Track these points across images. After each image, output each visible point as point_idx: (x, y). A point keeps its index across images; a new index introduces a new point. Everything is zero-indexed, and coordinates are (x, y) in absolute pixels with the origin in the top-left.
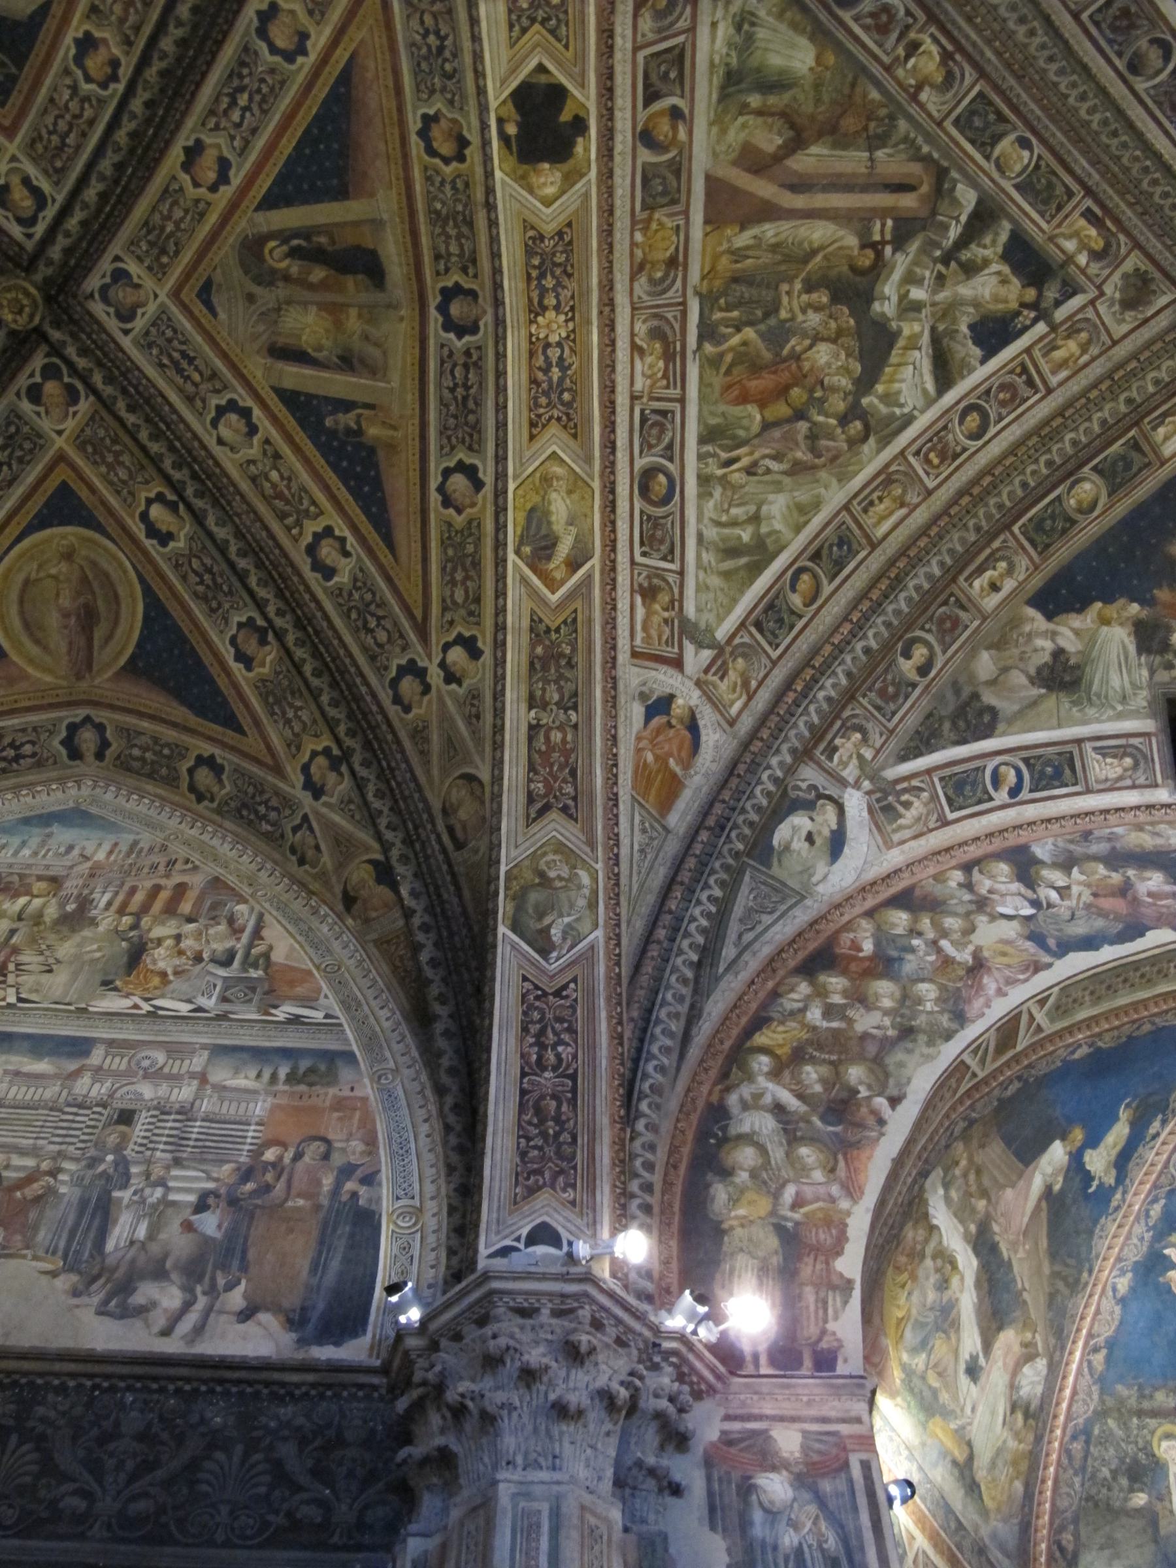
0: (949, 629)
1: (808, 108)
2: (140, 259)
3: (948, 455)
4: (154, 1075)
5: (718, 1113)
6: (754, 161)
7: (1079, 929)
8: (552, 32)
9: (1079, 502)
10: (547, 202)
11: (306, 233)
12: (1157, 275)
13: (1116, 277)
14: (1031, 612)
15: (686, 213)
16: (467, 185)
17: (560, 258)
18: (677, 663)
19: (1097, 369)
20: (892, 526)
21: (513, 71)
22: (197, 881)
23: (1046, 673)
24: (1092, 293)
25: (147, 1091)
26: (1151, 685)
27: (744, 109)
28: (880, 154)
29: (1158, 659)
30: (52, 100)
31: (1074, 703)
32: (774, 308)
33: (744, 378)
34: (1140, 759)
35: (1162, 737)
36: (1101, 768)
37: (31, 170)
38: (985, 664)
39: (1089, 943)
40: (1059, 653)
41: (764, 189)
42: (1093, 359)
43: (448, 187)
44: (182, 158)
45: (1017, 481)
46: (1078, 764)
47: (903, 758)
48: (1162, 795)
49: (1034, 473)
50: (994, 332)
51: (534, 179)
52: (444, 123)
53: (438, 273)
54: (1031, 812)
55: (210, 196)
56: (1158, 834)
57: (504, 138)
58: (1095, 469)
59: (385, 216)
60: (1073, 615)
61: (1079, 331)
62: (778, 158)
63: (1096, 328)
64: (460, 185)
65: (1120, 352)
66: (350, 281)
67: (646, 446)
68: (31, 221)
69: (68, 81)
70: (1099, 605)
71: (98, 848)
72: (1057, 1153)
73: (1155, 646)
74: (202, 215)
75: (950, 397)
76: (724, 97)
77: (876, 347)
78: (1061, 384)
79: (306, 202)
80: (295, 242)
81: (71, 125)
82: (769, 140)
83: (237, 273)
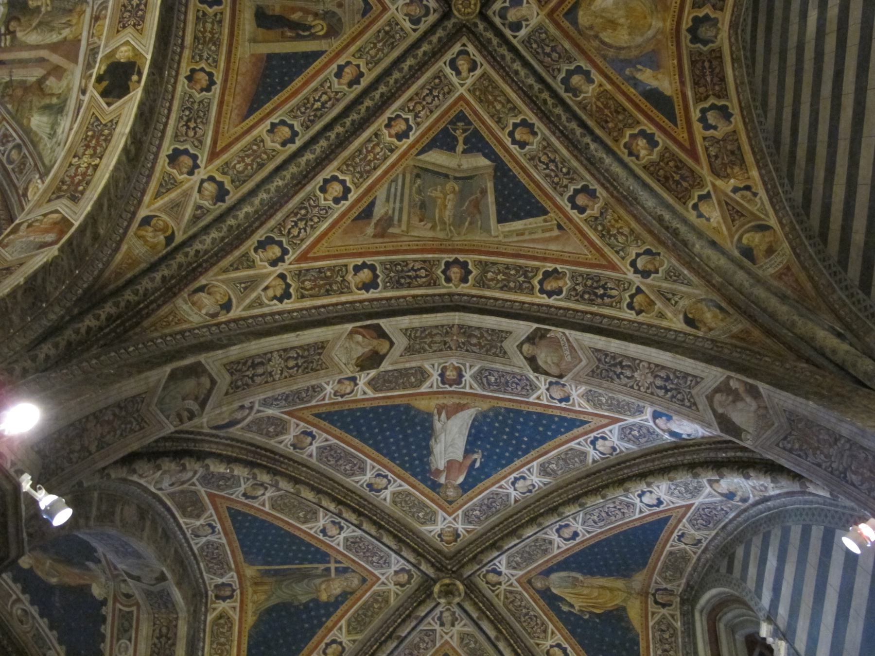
1: (35, 99)
2: (402, 29)
6: (57, 71)
8: (97, 119)
10: (127, 43)
11: (299, 38)
15: (88, 45)
16: (193, 57)
17: (127, 14)
21: (125, 103)
27: (59, 96)
28: (8, 79)
30: (431, 112)
37: (455, 79)
41: (55, 59)
43: (205, 55)
44: (362, 80)
51: (130, 54)
52: (198, 87)
53: (222, 13)
55: (351, 59)
57: (140, 74)
59: (247, 44)
62: (49, 74)
64: (198, 58)
66: (277, 11)
68: (460, 53)
69: (419, 120)
74: (359, 50)
76: (65, 101)
79: (296, 53)
80: (306, 33)
81: (424, 99)
82: (51, 82)
83: (345, 19)
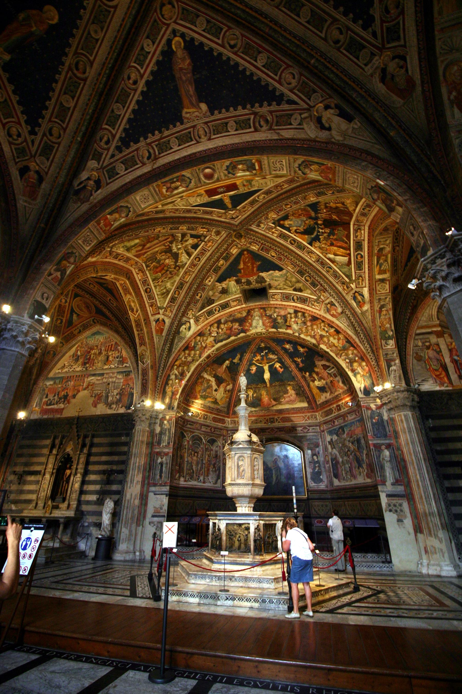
0: (204, 289)
3: (195, 266)
4: (111, 377)
5: (169, 376)
7: (221, 338)
18: (159, 313)
19: (216, 245)
20: (189, 279)
22: (114, 343)
25: (110, 380)
32: (156, 259)
33: (155, 270)
36: (233, 304)
38: (211, 293)
39: (221, 341)
40: (223, 288)
47: (199, 311)
48: (244, 306)
50: (195, 247)
54: (222, 313)
63: (213, 240)
65: (219, 241)
67: (144, 286)
71: (101, 338)
72: (227, 362)
75: (192, 258)
77: (176, 256)
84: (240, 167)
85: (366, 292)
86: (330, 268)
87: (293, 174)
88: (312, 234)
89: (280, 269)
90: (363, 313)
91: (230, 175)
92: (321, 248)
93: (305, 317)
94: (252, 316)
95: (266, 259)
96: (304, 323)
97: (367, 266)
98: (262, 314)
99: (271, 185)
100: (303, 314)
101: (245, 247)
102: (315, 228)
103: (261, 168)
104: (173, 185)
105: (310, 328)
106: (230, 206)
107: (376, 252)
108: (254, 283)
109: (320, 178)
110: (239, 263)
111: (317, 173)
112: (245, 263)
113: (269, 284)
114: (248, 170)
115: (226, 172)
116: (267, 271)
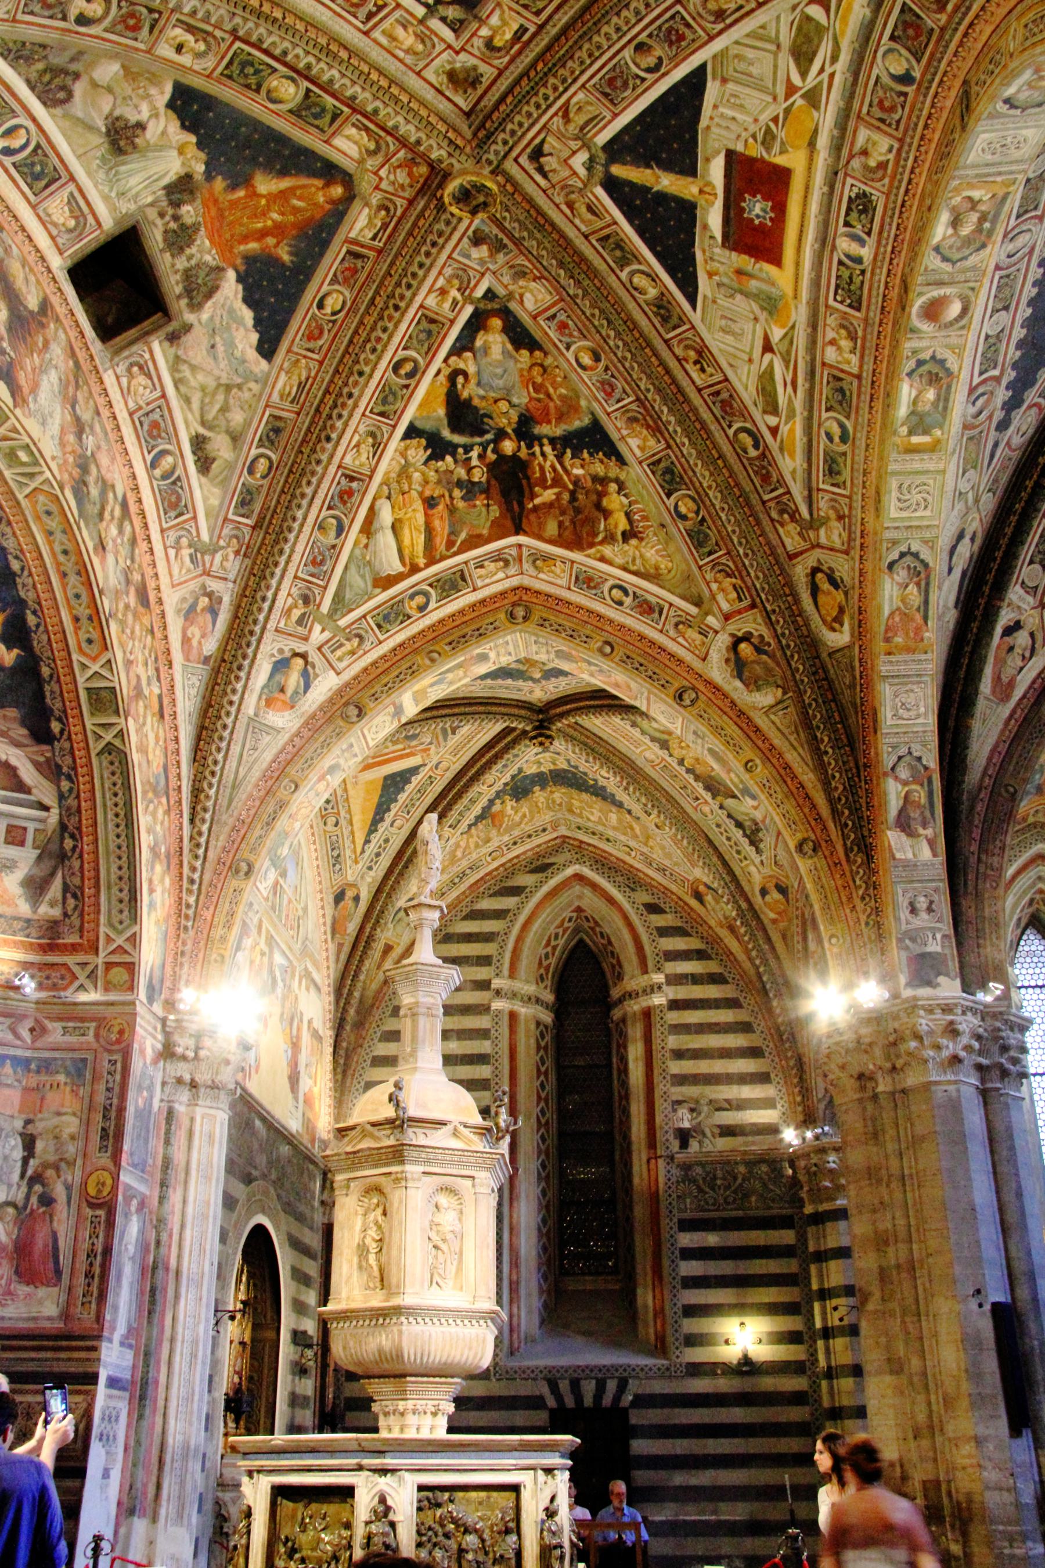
9: (276, 89)
12: (480, 92)
13: (474, 61)
14: (169, 89)
23: (120, 124)
24: (457, 46)
26: (141, 209)
29: (165, 204)
31: (103, 158)
34: (77, 232)
35: (103, 239)
36: (57, 207)
40: (141, 126)
42: (401, 61)
45: (286, 44)
46: (53, 188)
49: (297, 56)
56: (27, 280)
58: (308, 90)
60: (178, 123)
61: (423, 42)
70: (193, 139)
73: (175, 197)
78: (375, 41)
84: (931, 395)
85: (326, 685)
86: (340, 530)
87: (888, 535)
88: (455, 428)
89: (267, 348)
90: (256, 725)
91: (911, 364)
92: (404, 473)
93: (133, 560)
94: (46, 343)
95: (308, 278)
96: (128, 582)
97: (400, 638)
98: (68, 382)
99: (716, 342)
100: (133, 542)
101: (365, 184)
102: (482, 433)
103: (913, 450)
104: (974, 217)
105: (130, 617)
106: (617, 170)
107: (479, 651)
108: (181, 263)
109: (886, 612)
110: (283, 173)
111: (897, 603)
112: (283, 195)
113: (188, 328)
114: (913, 413)
115: (926, 355)
116: (248, 300)
